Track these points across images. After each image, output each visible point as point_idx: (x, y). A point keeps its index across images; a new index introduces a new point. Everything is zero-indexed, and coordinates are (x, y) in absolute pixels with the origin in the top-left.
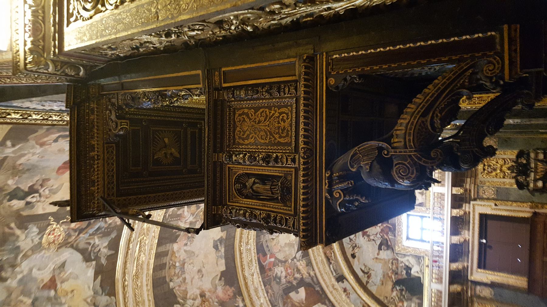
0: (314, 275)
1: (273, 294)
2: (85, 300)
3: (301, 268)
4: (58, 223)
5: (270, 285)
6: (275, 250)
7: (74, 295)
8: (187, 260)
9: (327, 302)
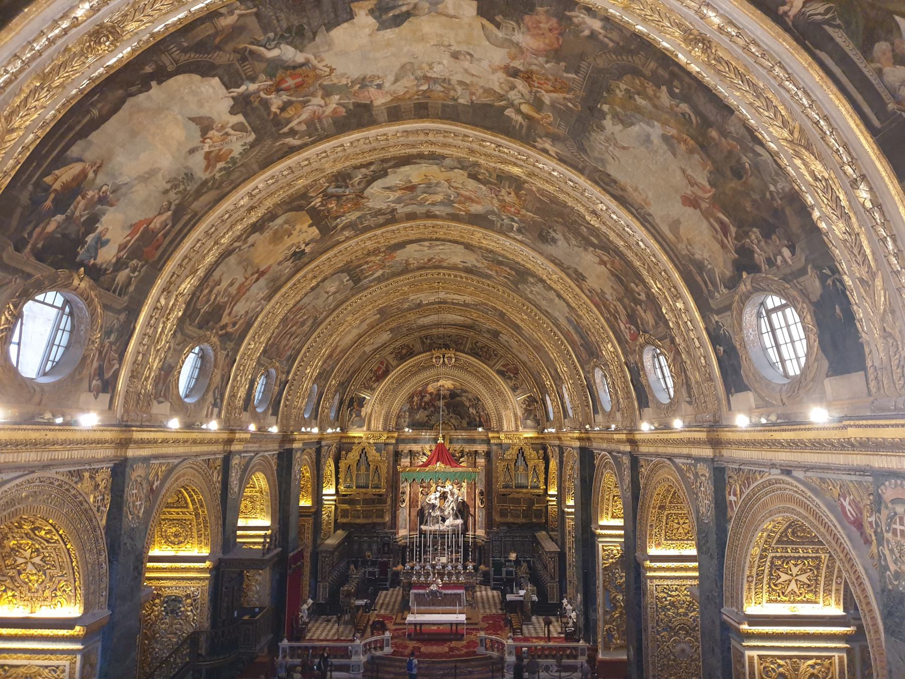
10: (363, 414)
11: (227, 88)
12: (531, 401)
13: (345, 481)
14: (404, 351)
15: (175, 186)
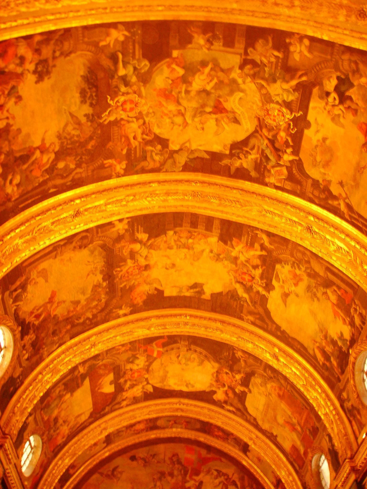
0: (122, 405)
1: (119, 353)
2: (189, 141)
3: (135, 389)
4: (292, 120)
5: (130, 349)
6: (164, 358)
7: (198, 129)
8: (191, 252)
9: (91, 420)
11: (267, 299)
15: (315, 295)
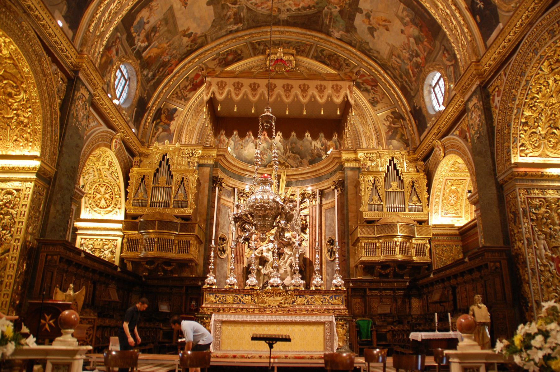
10: (172, 128)
12: (397, 117)
13: (136, 195)
14: (230, 57)
